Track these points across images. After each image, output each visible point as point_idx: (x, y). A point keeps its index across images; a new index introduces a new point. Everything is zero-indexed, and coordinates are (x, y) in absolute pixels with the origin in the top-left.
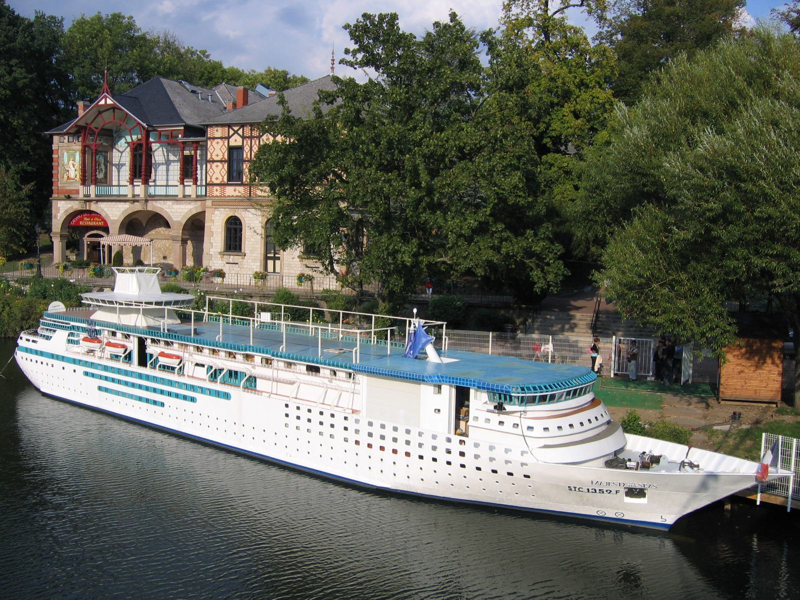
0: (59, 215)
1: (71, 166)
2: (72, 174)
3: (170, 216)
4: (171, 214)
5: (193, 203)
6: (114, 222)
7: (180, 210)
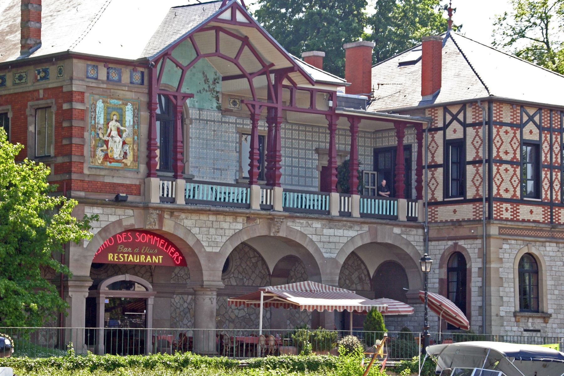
1: (114, 133)
3: (317, 249)
4: (320, 245)
5: (357, 228)
6: (211, 256)
7: (336, 239)
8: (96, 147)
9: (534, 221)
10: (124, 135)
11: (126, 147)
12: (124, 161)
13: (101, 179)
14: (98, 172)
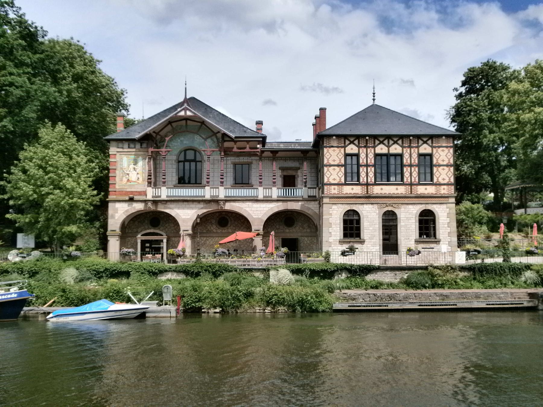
0: (117, 216)
2: (133, 176)
8: (123, 176)
9: (354, 193)
10: (137, 171)
11: (139, 176)
12: (138, 181)
13: (125, 190)
14: (124, 187)
